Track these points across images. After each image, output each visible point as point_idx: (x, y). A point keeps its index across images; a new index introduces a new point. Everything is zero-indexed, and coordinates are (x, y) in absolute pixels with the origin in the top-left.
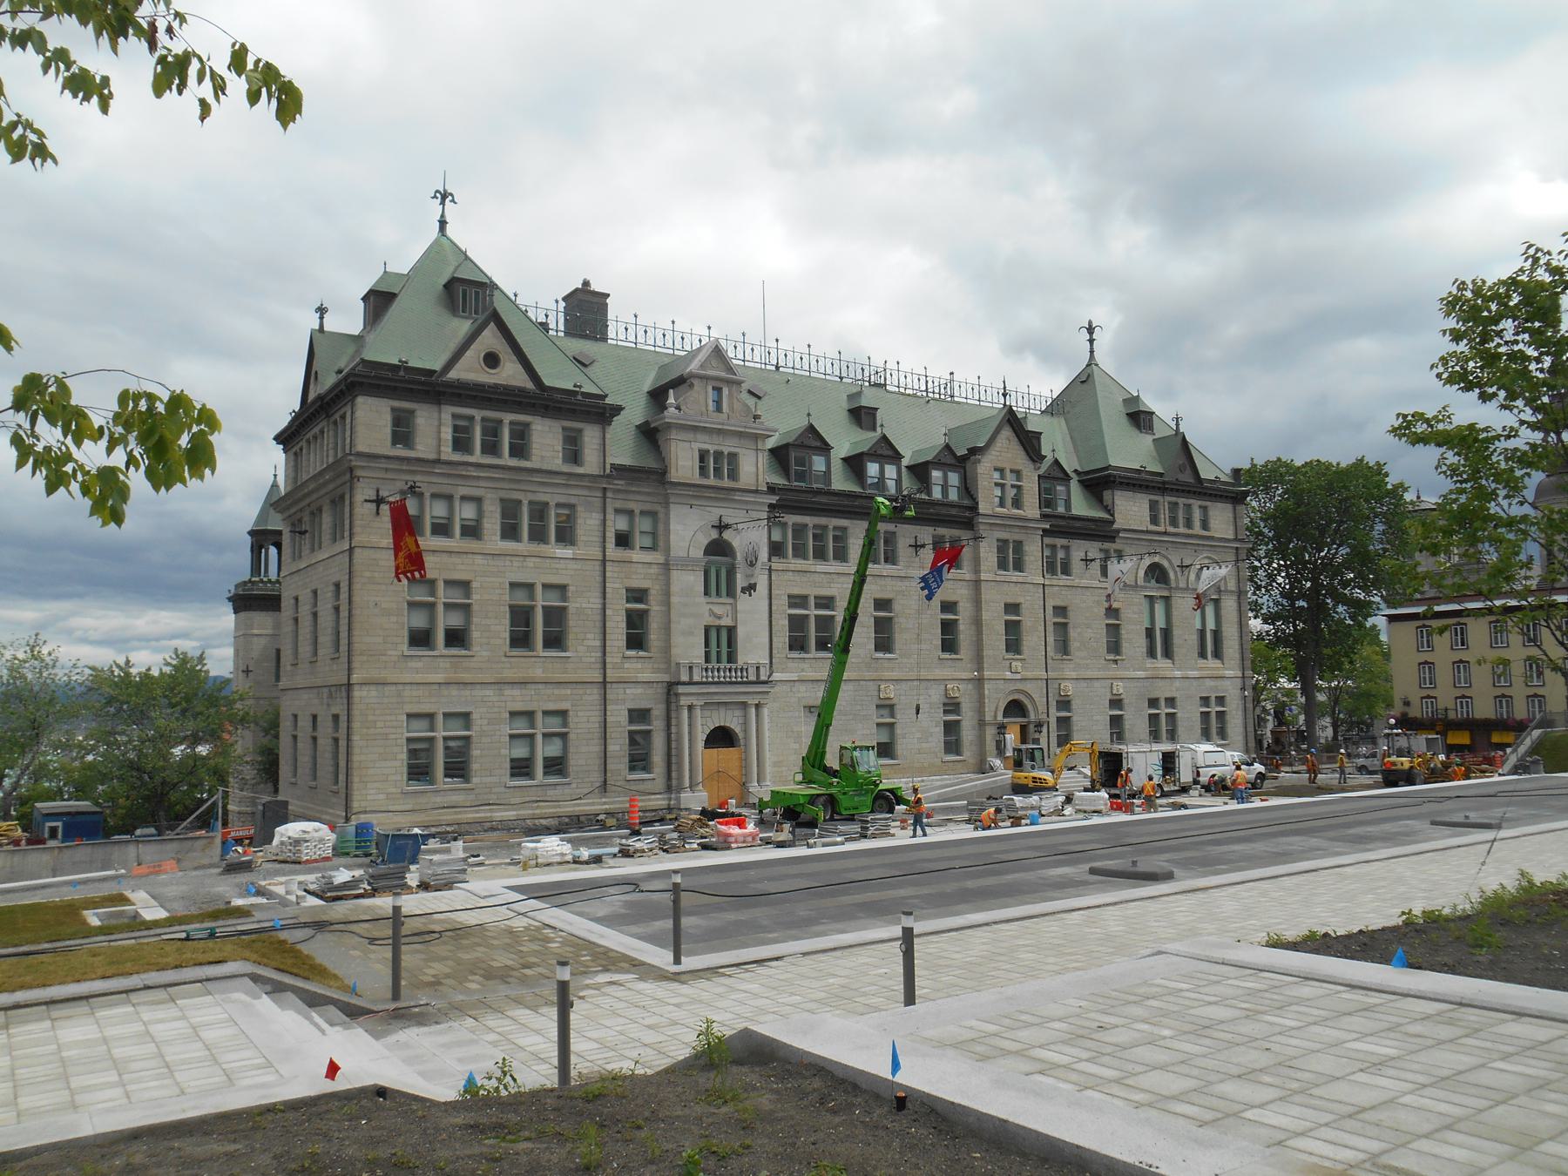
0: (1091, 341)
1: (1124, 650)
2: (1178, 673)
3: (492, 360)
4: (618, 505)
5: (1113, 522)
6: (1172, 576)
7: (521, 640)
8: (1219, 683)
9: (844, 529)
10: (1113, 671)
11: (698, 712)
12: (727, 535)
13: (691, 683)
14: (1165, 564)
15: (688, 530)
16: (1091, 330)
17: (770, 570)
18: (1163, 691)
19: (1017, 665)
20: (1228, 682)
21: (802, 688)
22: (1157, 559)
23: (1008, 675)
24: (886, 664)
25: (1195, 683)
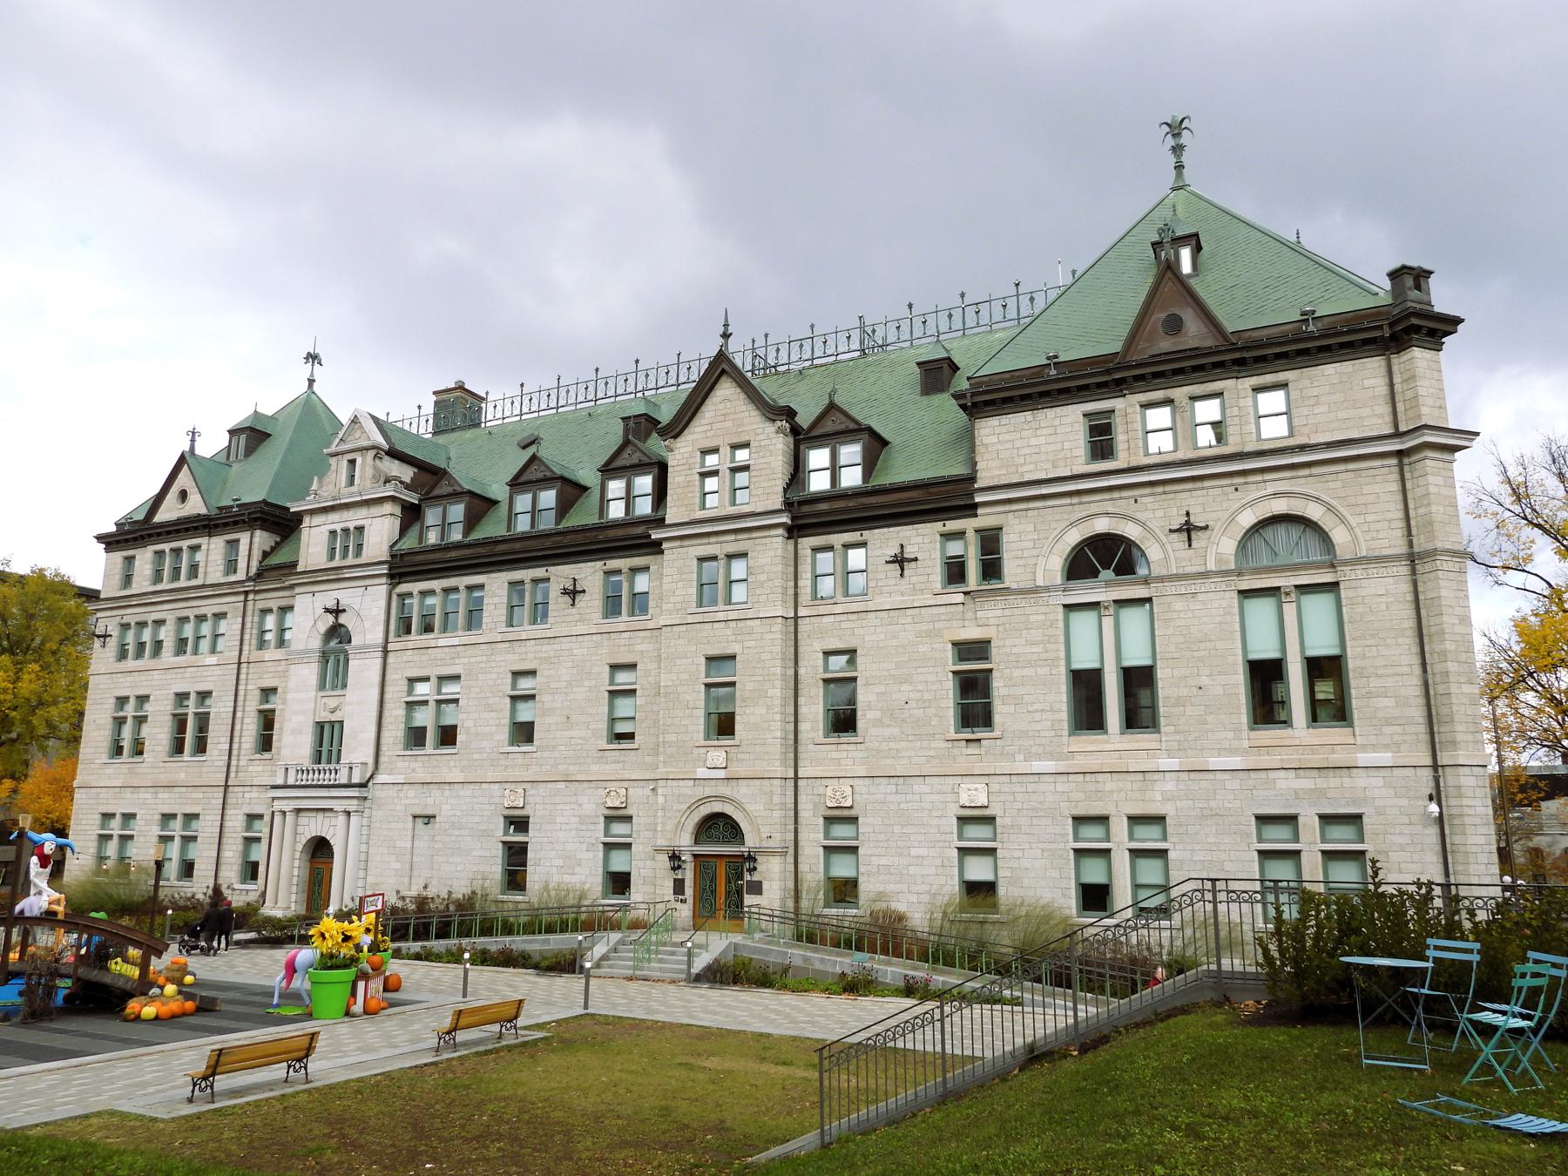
0: (1178, 149)
1: (997, 719)
2: (1174, 763)
3: (183, 495)
4: (260, 605)
5: (972, 479)
6: (1153, 552)
7: (178, 747)
8: (1333, 781)
9: (481, 587)
10: (966, 758)
11: (290, 818)
12: (343, 619)
13: (285, 787)
14: (1131, 531)
15: (307, 617)
16: (1176, 129)
17: (386, 652)
18: (1119, 802)
19: (717, 756)
20: (1361, 780)
21: (411, 792)
22: (1102, 526)
23: (702, 772)
24: (520, 760)
25: (1233, 783)
